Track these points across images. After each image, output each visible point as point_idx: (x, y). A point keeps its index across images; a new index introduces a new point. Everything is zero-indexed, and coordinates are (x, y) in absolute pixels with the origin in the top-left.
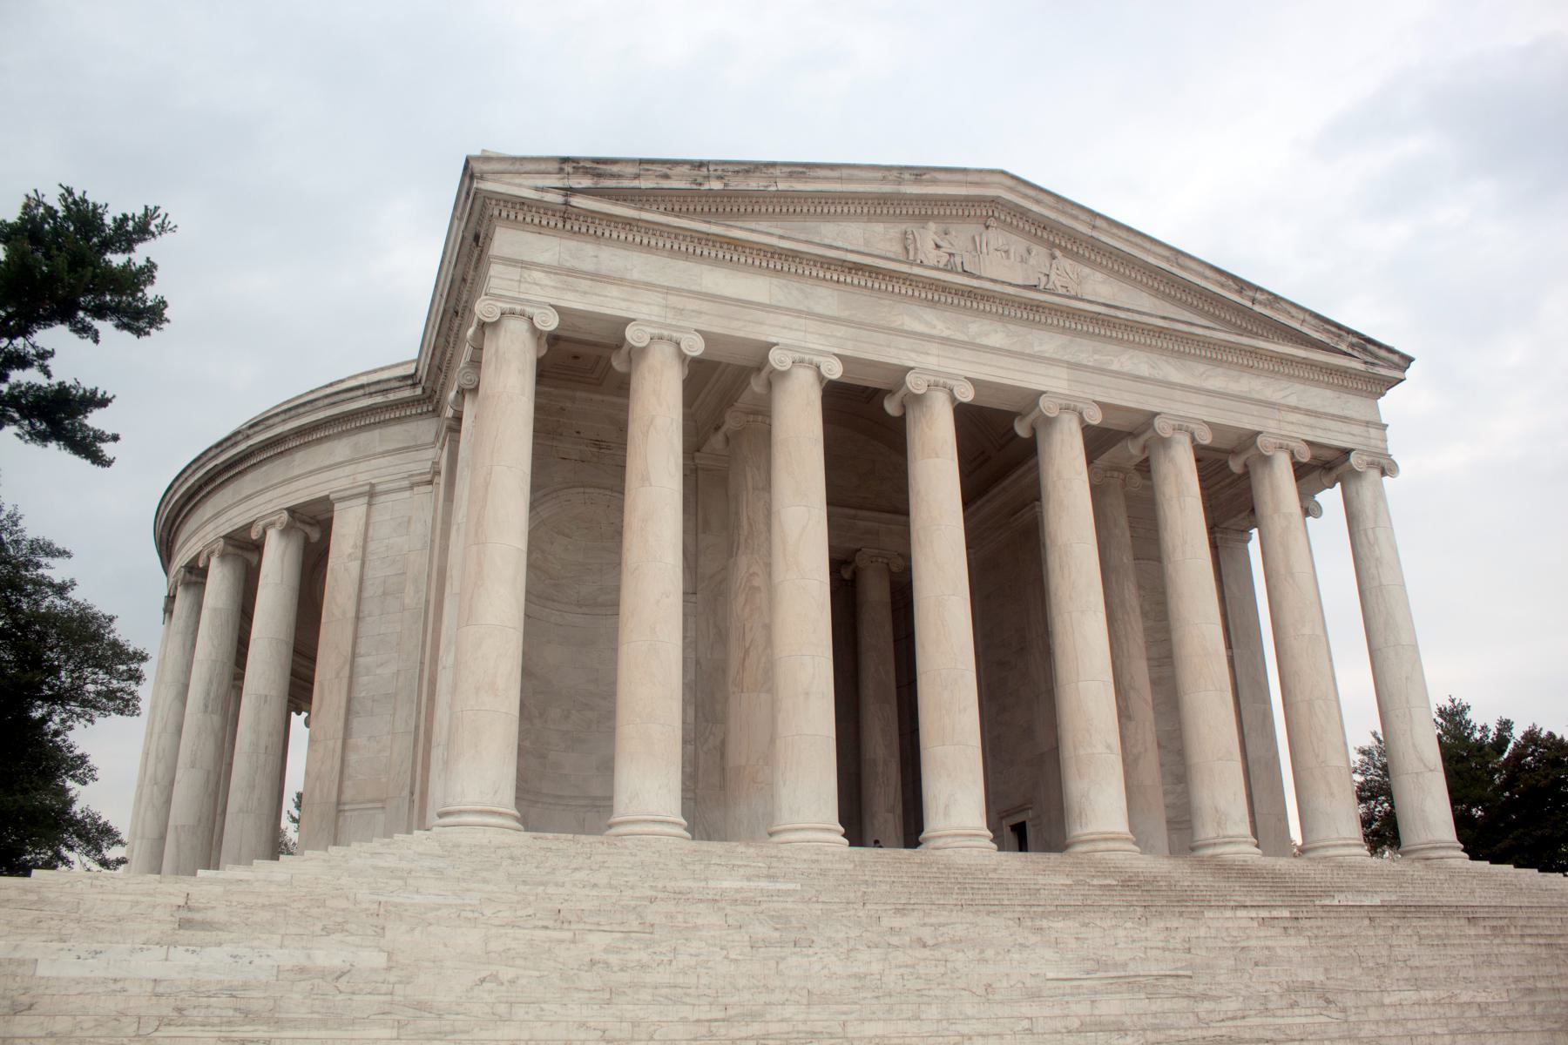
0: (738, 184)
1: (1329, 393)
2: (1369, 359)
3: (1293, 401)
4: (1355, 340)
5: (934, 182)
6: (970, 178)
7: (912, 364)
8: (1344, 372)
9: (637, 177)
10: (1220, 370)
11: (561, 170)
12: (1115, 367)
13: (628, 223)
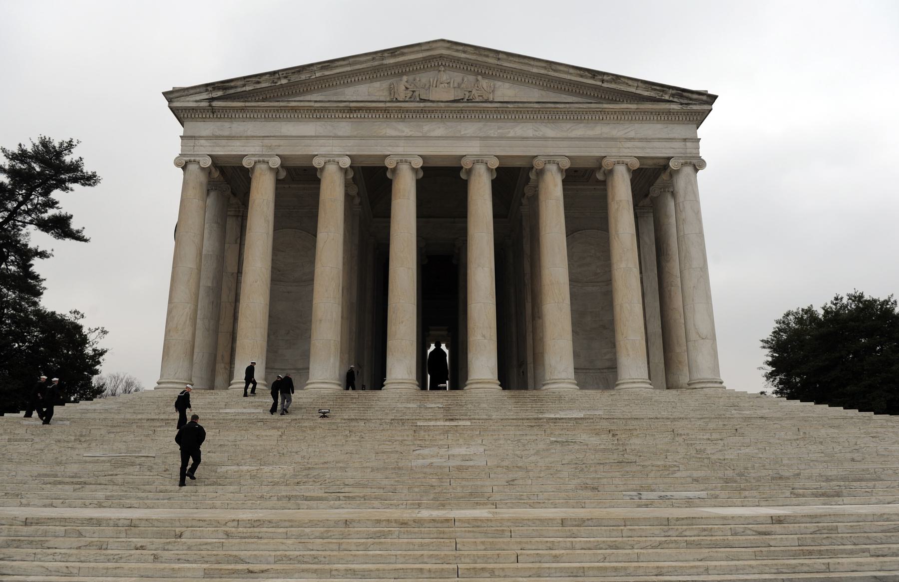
0: (294, 78)
1: (659, 126)
2: (686, 101)
3: (632, 134)
4: (674, 92)
5: (403, 54)
6: (423, 48)
7: (388, 153)
8: (669, 112)
9: (244, 85)
10: (582, 125)
11: (207, 90)
12: (510, 135)
13: (242, 109)
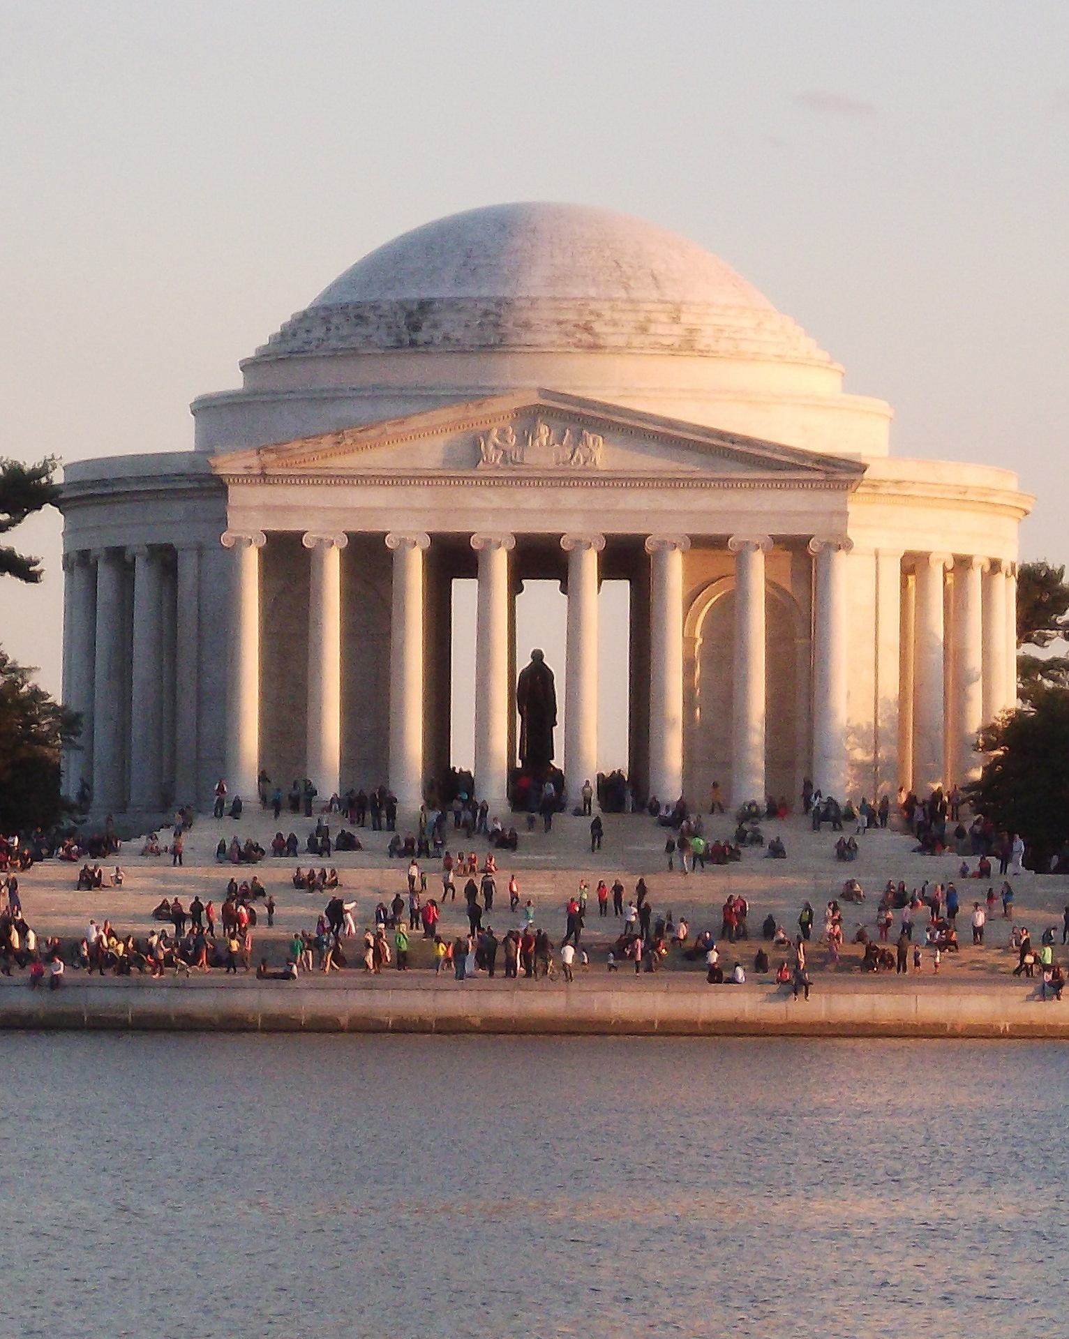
10: (707, 492)
12: (621, 506)
